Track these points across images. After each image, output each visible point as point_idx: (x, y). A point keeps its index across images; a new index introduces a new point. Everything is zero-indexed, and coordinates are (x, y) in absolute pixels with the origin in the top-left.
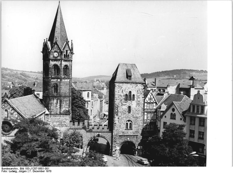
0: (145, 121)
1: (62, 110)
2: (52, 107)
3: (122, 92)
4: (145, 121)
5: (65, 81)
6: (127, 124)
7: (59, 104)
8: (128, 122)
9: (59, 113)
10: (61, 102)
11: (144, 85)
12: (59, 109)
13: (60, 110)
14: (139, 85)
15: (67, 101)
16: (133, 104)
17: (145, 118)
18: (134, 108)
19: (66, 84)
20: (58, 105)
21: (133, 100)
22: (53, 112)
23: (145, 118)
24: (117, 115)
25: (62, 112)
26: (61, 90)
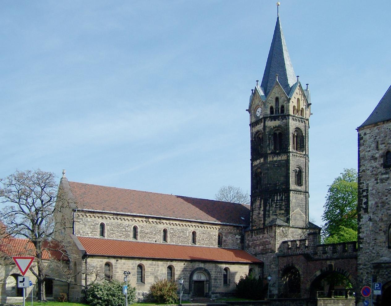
5: (275, 159)
7: (262, 208)
9: (262, 227)
13: (265, 220)
24: (366, 210)
26: (264, 180)
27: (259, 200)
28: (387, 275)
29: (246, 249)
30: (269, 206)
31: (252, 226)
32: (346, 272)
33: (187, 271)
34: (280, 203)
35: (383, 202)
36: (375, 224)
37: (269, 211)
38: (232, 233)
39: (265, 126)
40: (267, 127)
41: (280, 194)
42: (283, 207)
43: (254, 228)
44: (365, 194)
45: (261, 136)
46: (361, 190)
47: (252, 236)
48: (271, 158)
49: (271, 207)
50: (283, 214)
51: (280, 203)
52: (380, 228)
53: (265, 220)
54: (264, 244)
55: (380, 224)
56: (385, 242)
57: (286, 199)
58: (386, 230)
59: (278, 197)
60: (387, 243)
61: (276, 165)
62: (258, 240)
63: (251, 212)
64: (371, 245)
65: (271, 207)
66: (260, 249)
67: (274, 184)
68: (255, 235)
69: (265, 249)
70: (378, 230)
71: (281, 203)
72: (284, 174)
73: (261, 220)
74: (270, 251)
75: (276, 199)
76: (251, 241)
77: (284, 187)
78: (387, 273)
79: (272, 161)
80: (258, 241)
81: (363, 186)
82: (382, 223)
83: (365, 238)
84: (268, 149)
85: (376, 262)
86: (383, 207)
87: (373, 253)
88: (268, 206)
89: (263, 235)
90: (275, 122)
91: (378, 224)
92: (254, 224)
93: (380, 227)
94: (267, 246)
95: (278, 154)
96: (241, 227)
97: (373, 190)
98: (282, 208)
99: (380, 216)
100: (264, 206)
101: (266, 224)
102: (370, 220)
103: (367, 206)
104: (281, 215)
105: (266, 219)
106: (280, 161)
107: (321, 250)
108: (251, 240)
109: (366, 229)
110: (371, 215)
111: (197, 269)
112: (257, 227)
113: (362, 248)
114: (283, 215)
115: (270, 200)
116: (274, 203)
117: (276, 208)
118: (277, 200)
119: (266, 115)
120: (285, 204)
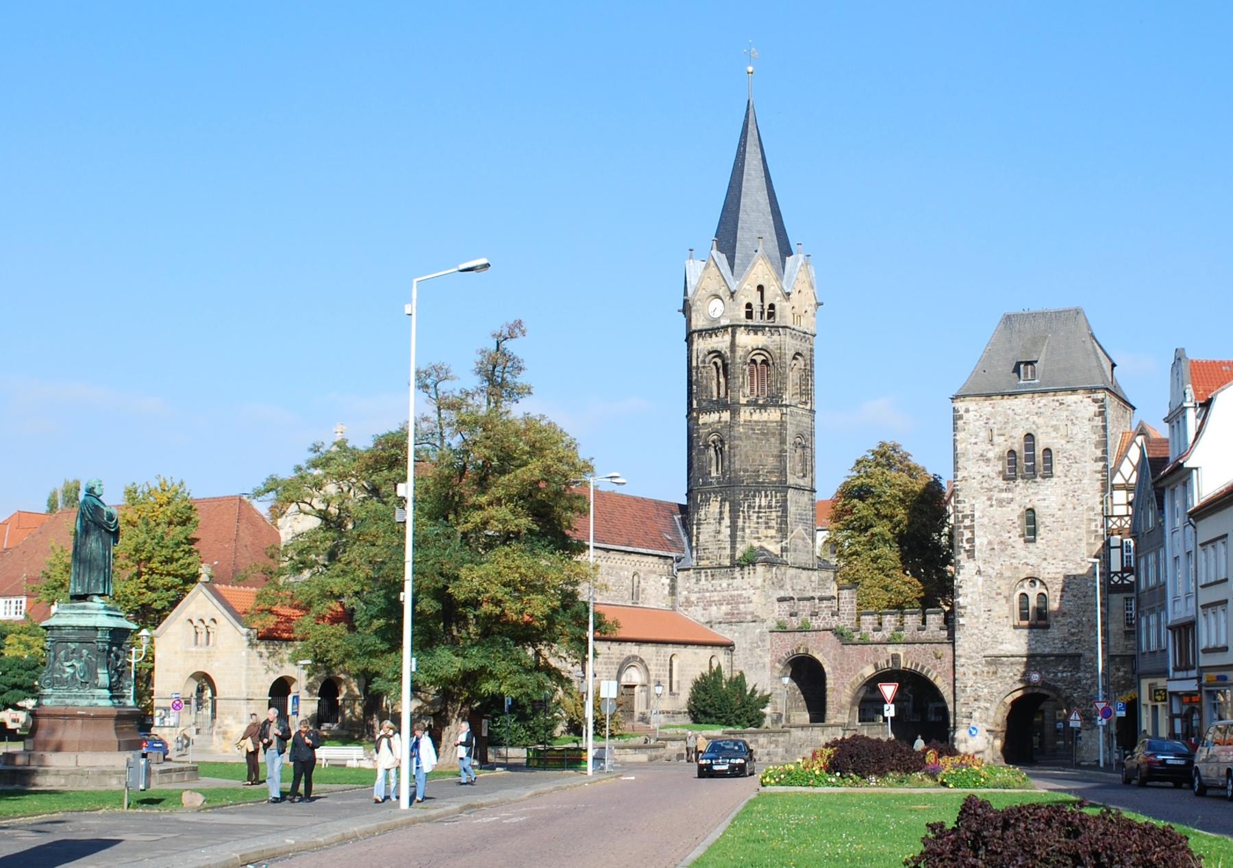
1: (741, 549)
2: (701, 537)
4: (1116, 579)
5: (756, 417)
6: (1024, 596)
7: (727, 522)
8: (1026, 588)
9: (727, 562)
11: (1100, 396)
12: (728, 546)
13: (733, 548)
14: (1070, 399)
17: (1116, 566)
18: (1053, 516)
19: (763, 434)
21: (1044, 477)
22: (708, 558)
23: (1116, 566)
24: (971, 554)
25: (738, 555)
26: (733, 460)
27: (716, 501)
28: (1011, 677)
29: (682, 608)
30: (744, 518)
31: (699, 558)
33: (612, 663)
34: (765, 512)
36: (989, 582)
37: (743, 529)
38: (655, 572)
39: (733, 345)
40: (739, 346)
41: (765, 493)
42: (773, 523)
43: (702, 563)
44: (967, 522)
46: (960, 515)
47: (698, 580)
49: (747, 521)
50: (772, 537)
51: (765, 512)
52: (999, 591)
53: (733, 548)
54: (733, 601)
55: (998, 583)
56: (1007, 617)
57: (778, 505)
58: (1010, 595)
59: (763, 499)
60: (1011, 619)
61: (758, 430)
62: (715, 590)
63: (695, 527)
64: (981, 620)
65: (747, 521)
66: (722, 612)
67: (754, 472)
68: (706, 580)
69: (736, 612)
70: (993, 594)
71: (767, 514)
72: (776, 452)
73: (725, 548)
74: (749, 617)
75: (757, 504)
76: (696, 592)
77: (774, 479)
78: (1011, 674)
79: (750, 421)
80: (715, 593)
81: (964, 507)
83: (969, 607)
84: (741, 393)
85: (989, 652)
86: (1002, 551)
87: (984, 636)
88: (741, 517)
89: (731, 581)
90: (756, 336)
91: (995, 583)
92: (701, 553)
93: (999, 588)
94: (742, 606)
95: (764, 407)
96: (672, 558)
97: (983, 517)
98: (770, 524)
99: (998, 567)
101: (737, 558)
102: (979, 572)
103: (974, 546)
104: (769, 539)
105: (738, 546)
106: (766, 422)
107: (870, 624)
108: (696, 590)
109: (971, 590)
110: (980, 563)
111: (629, 659)
112: (711, 563)
113: (963, 625)
114: (773, 540)
115: (746, 505)
116: (754, 512)
117: (758, 523)
118: (760, 507)
119: (737, 320)
120: (777, 517)
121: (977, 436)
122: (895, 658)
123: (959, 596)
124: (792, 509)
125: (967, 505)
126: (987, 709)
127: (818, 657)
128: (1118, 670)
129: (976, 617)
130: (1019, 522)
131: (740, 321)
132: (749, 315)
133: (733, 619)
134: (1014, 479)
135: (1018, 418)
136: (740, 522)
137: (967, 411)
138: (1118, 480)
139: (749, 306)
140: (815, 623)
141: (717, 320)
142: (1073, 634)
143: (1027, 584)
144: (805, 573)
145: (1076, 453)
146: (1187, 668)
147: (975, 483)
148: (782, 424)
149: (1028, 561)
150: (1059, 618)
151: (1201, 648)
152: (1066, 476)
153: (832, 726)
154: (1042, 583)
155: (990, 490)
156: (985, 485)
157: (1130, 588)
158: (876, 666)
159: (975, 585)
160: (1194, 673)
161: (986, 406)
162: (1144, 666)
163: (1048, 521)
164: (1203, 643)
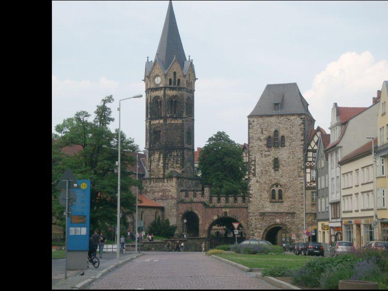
0: (308, 185)
1: (168, 172)
2: (152, 167)
3: (262, 132)
5: (173, 122)
6: (274, 191)
7: (161, 161)
8: (275, 188)
9: (161, 176)
10: (165, 158)
11: (303, 117)
12: (162, 170)
13: (164, 171)
14: (292, 118)
15: (178, 156)
16: (283, 154)
17: (308, 180)
20: (160, 164)
23: (308, 180)
24: (254, 175)
28: (269, 221)
30: (168, 160)
32: (238, 218)
35: (266, 171)
37: (168, 164)
39: (164, 94)
43: (152, 177)
44: (253, 163)
45: (159, 100)
47: (150, 183)
48: (170, 121)
50: (179, 167)
54: (164, 191)
60: (269, 199)
82: (266, 185)
94: (167, 193)
95: (176, 118)
99: (264, 180)
100: (163, 160)
102: (257, 182)
113: (251, 201)
117: (173, 162)
118: (174, 156)
121: (257, 131)
122: (226, 213)
123: (249, 190)
124: (186, 157)
125: (253, 156)
126: (260, 232)
127: (196, 212)
128: (309, 218)
129: (256, 198)
130: (272, 163)
131: (167, 85)
132: (170, 83)
133: (163, 198)
134: (271, 147)
135: (272, 124)
136: (167, 162)
137: (253, 121)
138: (310, 148)
139: (170, 80)
140: (195, 200)
141: (157, 85)
142: (292, 205)
143: (275, 186)
144: (190, 182)
145: (294, 138)
146: (336, 218)
147: (256, 149)
148: (182, 124)
149: (276, 178)
150: (287, 199)
151: (342, 211)
152: (290, 146)
153: (201, 238)
154: (281, 186)
155: (262, 151)
156: (260, 149)
157: (314, 188)
158: (218, 216)
159: (256, 186)
160: (339, 220)
161: (261, 120)
162: (319, 217)
163: (283, 163)
164: (343, 209)
